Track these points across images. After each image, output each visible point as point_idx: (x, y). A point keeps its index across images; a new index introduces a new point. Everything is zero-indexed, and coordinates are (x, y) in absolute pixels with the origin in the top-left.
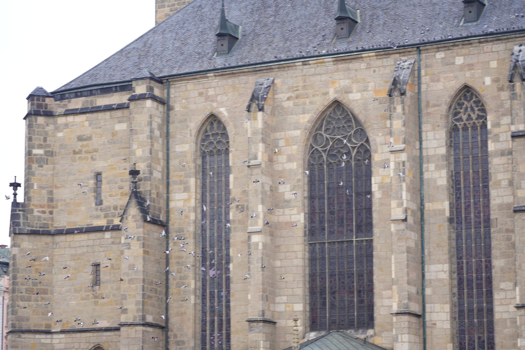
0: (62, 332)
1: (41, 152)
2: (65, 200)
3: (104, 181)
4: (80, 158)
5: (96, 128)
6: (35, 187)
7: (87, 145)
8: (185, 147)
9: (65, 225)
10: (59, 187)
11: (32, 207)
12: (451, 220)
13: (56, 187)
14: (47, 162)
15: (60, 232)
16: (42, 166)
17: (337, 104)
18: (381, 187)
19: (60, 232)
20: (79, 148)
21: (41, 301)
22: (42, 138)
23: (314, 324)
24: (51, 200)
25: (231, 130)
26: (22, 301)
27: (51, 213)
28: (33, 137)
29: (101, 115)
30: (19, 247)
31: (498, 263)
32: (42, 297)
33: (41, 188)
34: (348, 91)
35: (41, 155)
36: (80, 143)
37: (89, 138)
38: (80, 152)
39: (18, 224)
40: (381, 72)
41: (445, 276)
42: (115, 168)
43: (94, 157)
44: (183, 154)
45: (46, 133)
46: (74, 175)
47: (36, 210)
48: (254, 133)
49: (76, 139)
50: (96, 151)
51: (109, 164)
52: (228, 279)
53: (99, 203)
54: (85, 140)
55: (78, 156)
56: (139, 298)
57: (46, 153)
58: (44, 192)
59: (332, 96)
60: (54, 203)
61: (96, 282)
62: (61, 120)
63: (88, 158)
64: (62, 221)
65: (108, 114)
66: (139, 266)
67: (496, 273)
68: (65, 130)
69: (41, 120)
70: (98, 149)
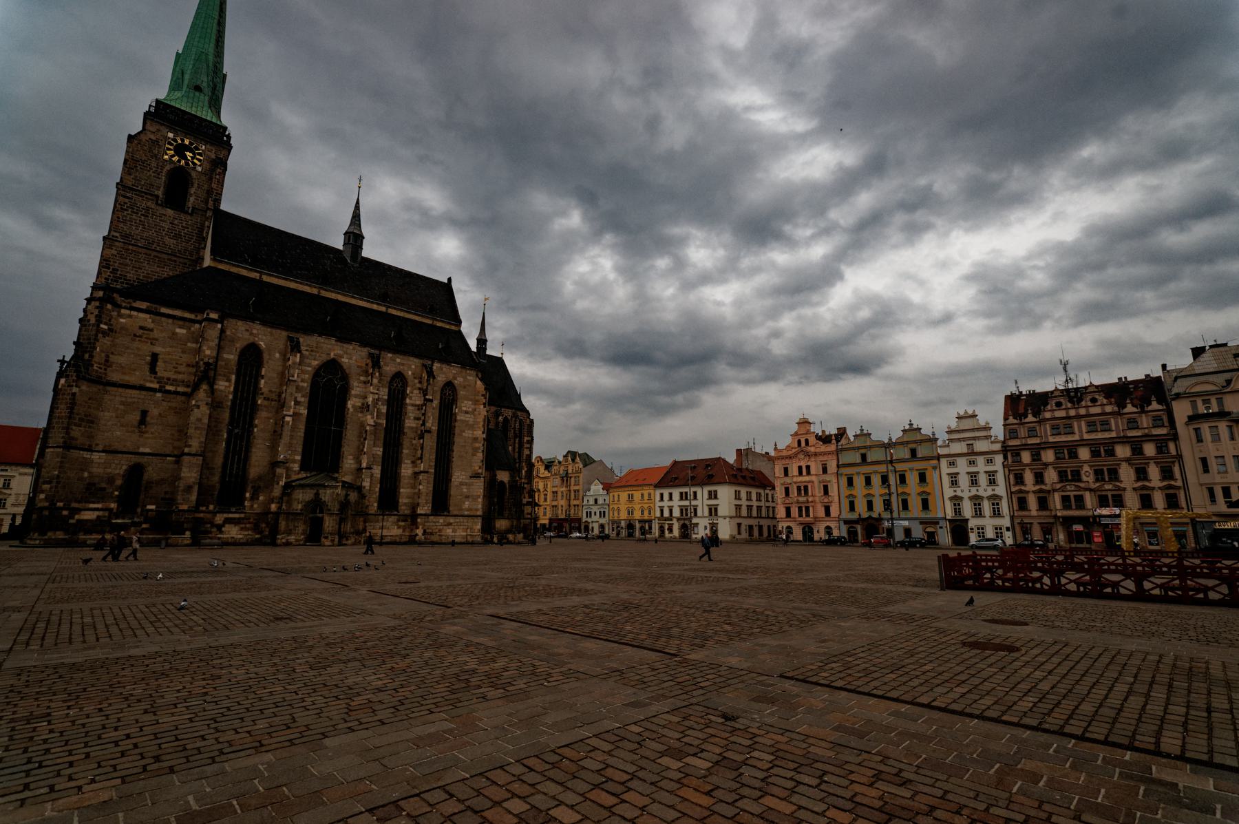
0: (103, 451)
8: (231, 357)
12: (386, 429)
15: (114, 384)
17: (333, 360)
18: (353, 406)
19: (114, 384)
23: (304, 466)
24: (107, 361)
25: (266, 356)
29: (163, 319)
31: (405, 451)
33: (101, 351)
34: (341, 357)
37: (152, 330)
41: (380, 453)
44: (229, 360)
48: (294, 363)
52: (249, 437)
53: (153, 370)
56: (203, 439)
59: (332, 355)
61: (143, 421)
62: (123, 311)
64: (115, 376)
65: (170, 321)
66: (206, 421)
67: (404, 456)
69: (109, 306)
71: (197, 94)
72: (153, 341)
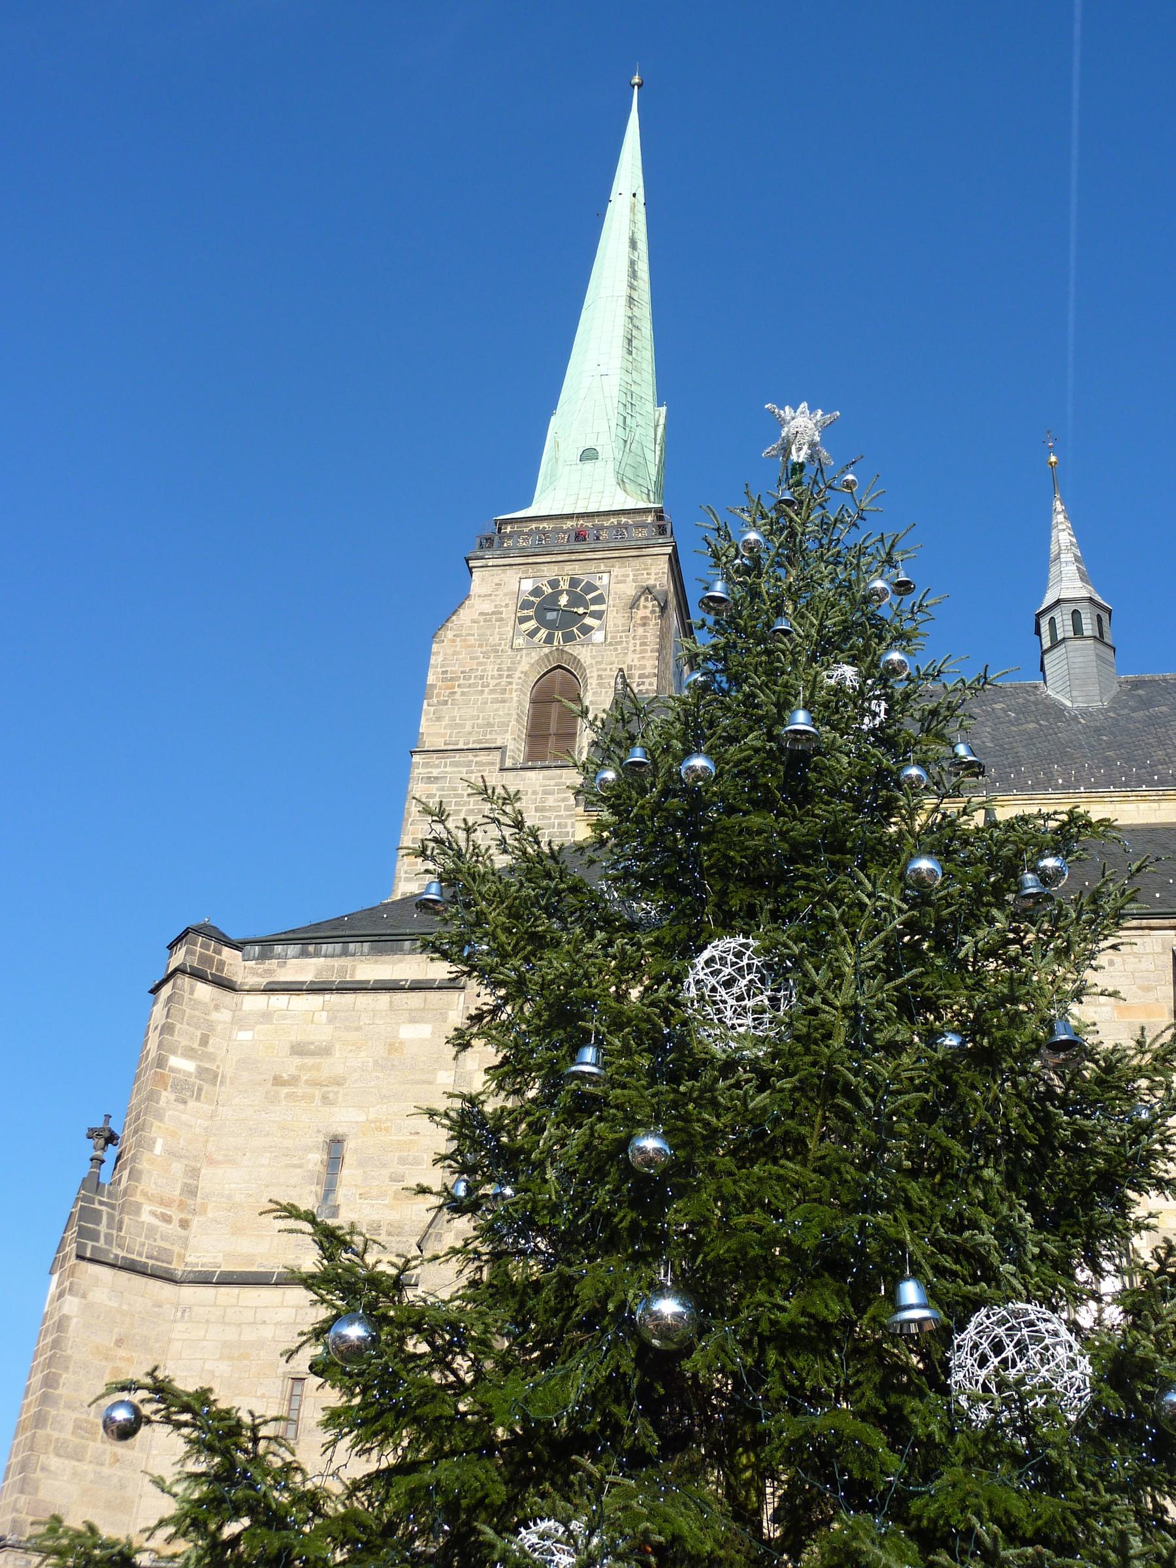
1: (189, 1066)
2: (229, 1197)
3: (349, 1158)
4: (288, 1096)
5: (347, 1029)
6: (158, 1149)
7: (316, 1067)
9: (220, 1260)
10: (218, 1162)
11: (138, 1198)
13: (211, 1162)
14: (199, 1095)
16: (185, 1102)
20: (293, 1071)
21: (111, 1465)
22: (198, 1033)
26: (58, 1455)
27: (184, 1224)
28: (179, 1026)
29: (363, 999)
30: (84, 1296)
32: (115, 1454)
33: (171, 1153)
35: (189, 1075)
36: (297, 1061)
37: (325, 1051)
38: (293, 1081)
39: (94, 1236)
40: (1129, 968)
42: (387, 1130)
43: (331, 1096)
45: (211, 1026)
46: (268, 1135)
47: (147, 1208)
49: (287, 1050)
50: (339, 1082)
51: (372, 1117)
54: (312, 1054)
55: (285, 1090)
57: (201, 1071)
58: (177, 1167)
60: (199, 1200)
62: (254, 1003)
63: (313, 1096)
65: (384, 998)
68: (259, 1027)
69: (204, 991)
70: (345, 1079)
71: (589, 466)
72: (329, 1090)
